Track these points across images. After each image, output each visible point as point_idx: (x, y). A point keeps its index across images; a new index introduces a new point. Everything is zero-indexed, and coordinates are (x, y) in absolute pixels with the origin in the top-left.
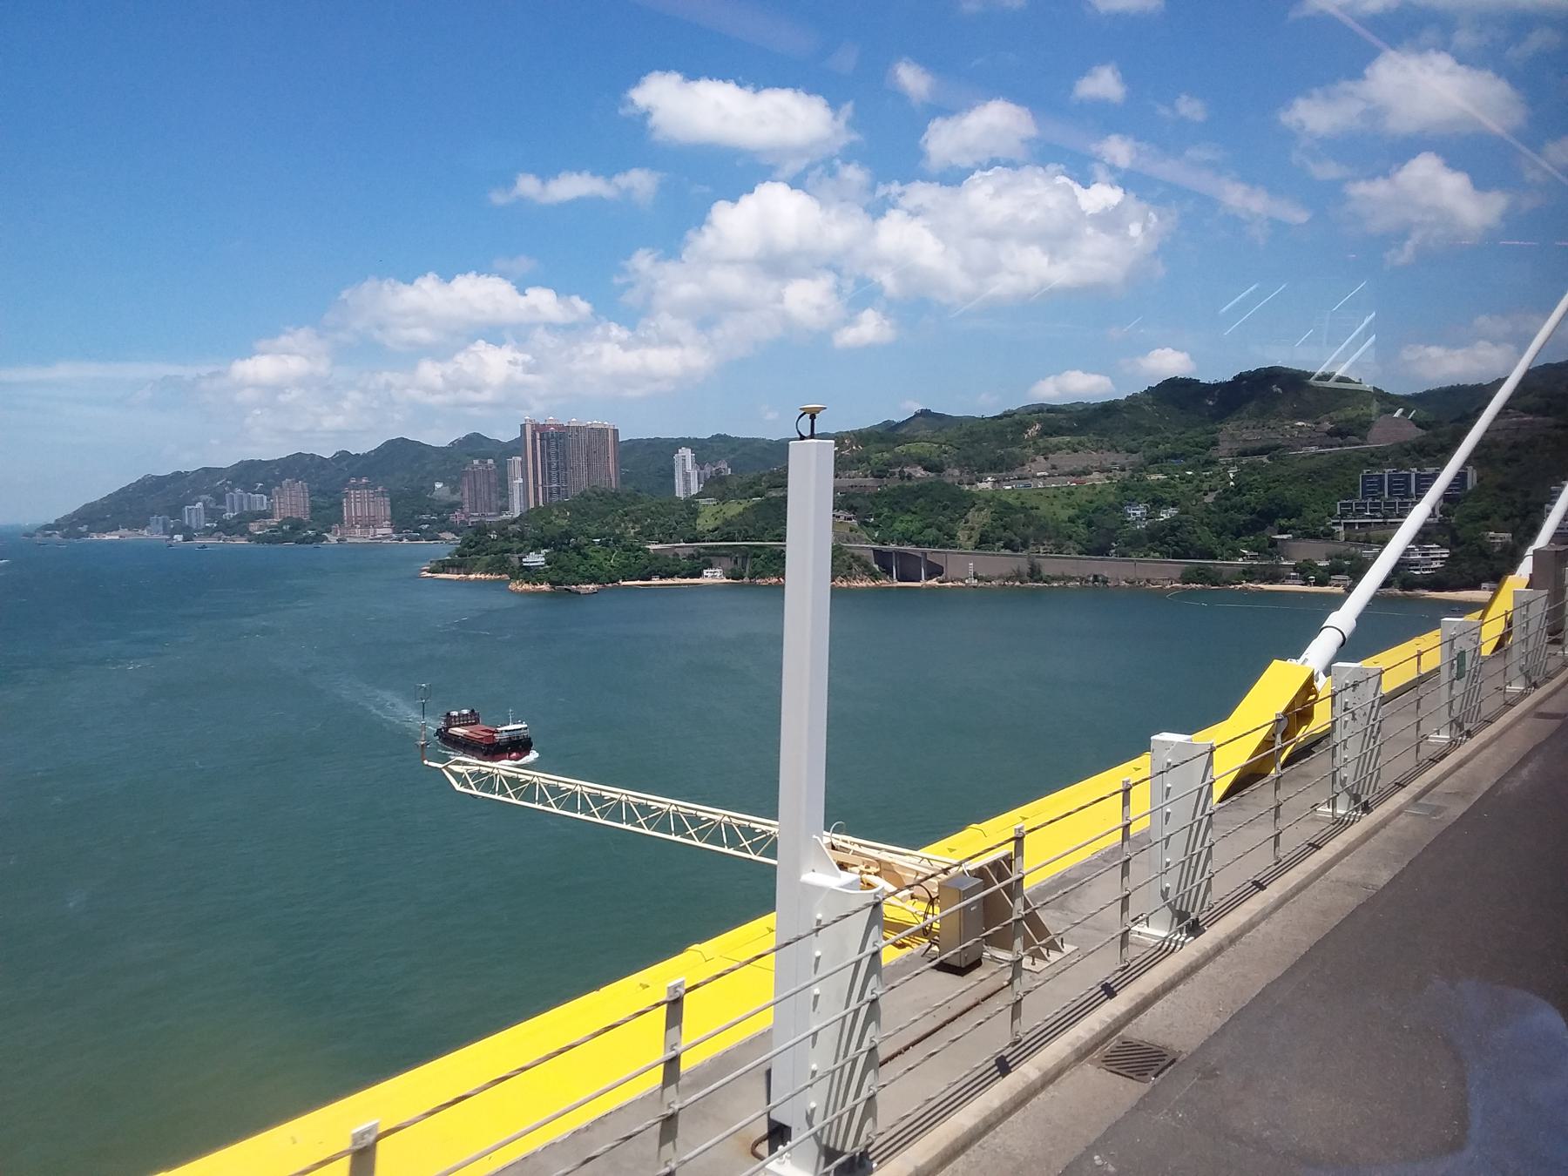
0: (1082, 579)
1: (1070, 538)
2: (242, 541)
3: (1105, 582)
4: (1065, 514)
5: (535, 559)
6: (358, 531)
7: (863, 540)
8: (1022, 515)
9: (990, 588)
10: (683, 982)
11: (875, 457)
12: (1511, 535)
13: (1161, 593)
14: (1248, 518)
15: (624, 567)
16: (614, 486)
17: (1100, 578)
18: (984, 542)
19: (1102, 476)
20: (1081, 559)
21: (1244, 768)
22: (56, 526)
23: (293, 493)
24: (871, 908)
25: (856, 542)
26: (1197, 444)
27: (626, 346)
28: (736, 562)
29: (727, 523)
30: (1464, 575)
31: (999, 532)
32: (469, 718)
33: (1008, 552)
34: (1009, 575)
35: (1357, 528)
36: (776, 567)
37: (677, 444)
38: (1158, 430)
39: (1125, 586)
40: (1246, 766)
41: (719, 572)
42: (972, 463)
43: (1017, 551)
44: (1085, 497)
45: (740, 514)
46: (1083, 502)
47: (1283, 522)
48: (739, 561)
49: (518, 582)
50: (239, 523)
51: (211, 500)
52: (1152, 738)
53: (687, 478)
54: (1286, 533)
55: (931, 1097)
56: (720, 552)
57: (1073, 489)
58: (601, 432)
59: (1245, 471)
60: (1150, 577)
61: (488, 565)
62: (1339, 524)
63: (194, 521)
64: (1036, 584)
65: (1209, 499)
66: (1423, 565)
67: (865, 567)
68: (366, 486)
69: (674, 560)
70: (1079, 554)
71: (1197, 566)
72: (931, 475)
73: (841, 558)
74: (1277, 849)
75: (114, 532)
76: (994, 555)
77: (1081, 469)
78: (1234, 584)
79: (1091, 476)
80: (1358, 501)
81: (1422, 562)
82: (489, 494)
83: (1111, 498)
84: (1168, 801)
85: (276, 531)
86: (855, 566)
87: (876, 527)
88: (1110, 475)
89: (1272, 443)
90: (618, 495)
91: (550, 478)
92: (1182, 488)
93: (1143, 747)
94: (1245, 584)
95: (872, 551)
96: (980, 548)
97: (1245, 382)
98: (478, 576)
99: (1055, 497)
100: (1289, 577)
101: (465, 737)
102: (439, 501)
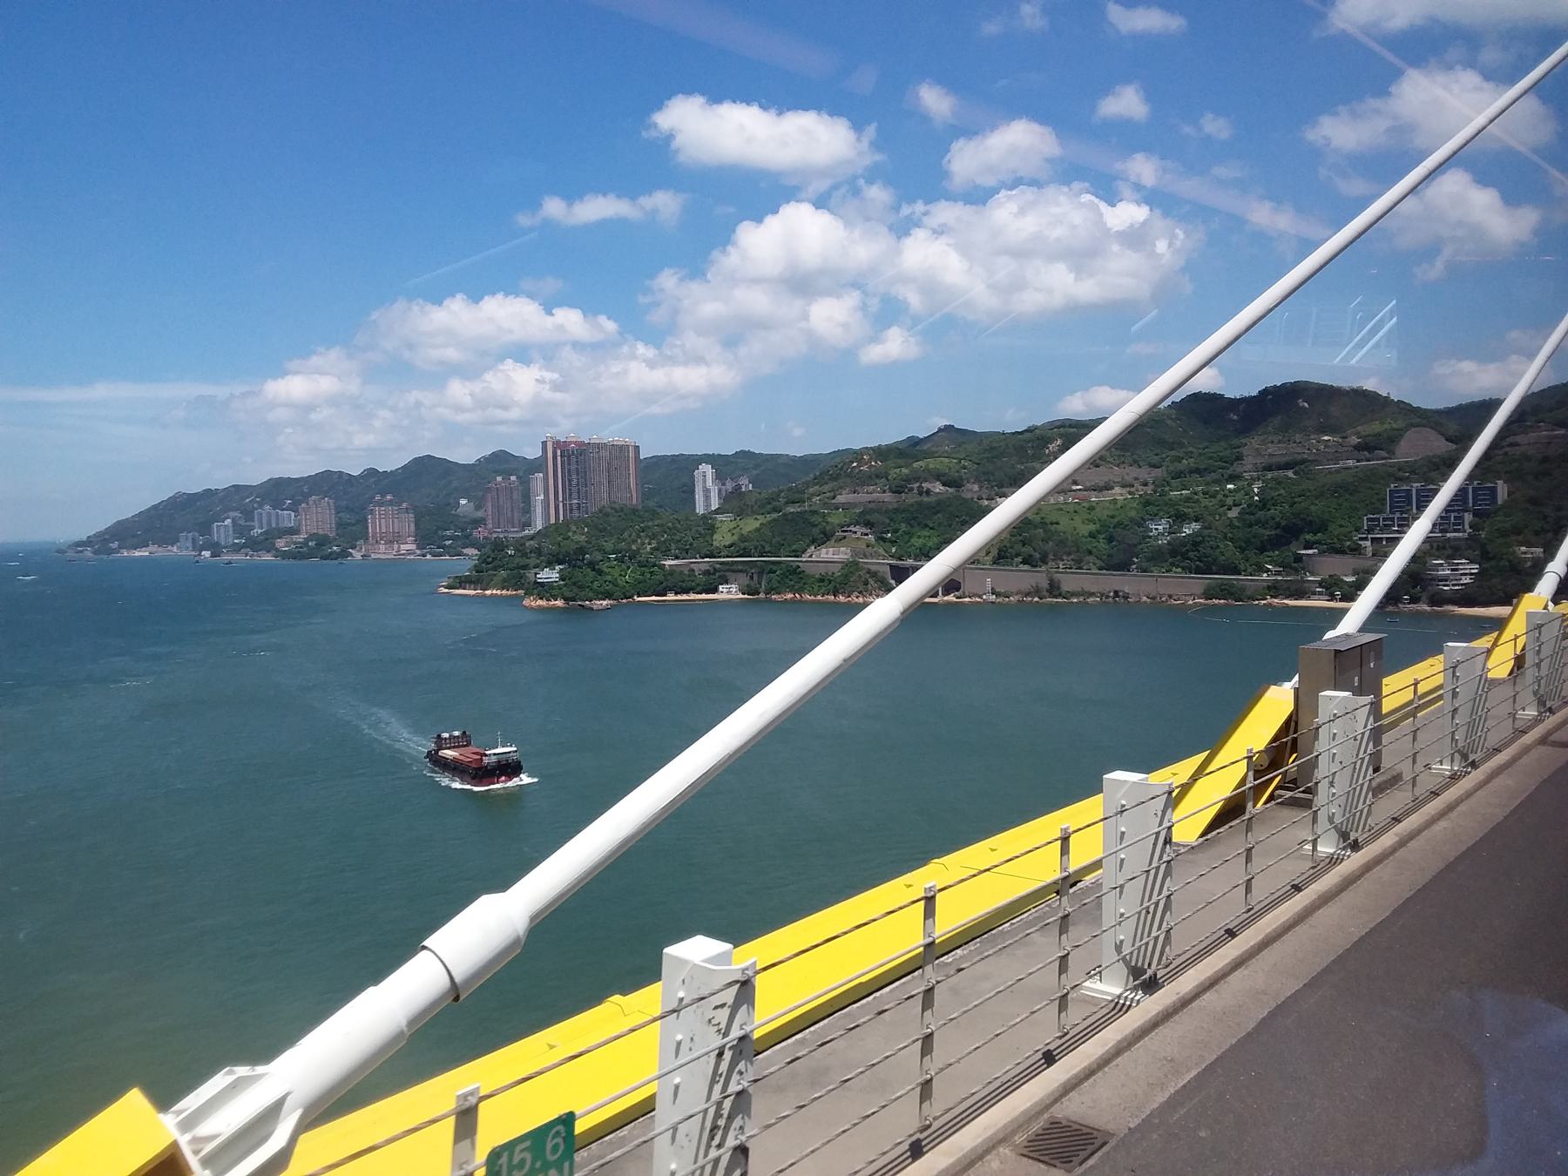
0: (1102, 595)
1: (1090, 553)
2: (268, 557)
3: (1126, 597)
4: (1085, 529)
5: (549, 575)
6: (382, 547)
7: (880, 556)
8: (1041, 530)
9: (1007, 603)
10: (478, 1088)
11: (894, 473)
13: (1184, 607)
14: (1272, 533)
15: (639, 583)
16: (634, 502)
17: (1121, 594)
19: (1124, 491)
20: (1101, 574)
21: (1228, 801)
22: (89, 542)
23: (320, 510)
24: (738, 985)
25: (872, 557)
27: (651, 364)
28: (752, 578)
29: (743, 539)
31: (1018, 547)
32: (460, 740)
33: (1026, 567)
34: (1028, 591)
35: (1384, 543)
36: (792, 583)
37: (697, 460)
38: (1182, 445)
39: (1145, 602)
41: (734, 588)
42: (992, 478)
43: (1036, 566)
44: (1106, 512)
45: (757, 530)
46: (1105, 517)
47: (1308, 537)
48: (755, 577)
49: (532, 598)
50: (267, 539)
51: (240, 517)
52: (1104, 776)
53: (707, 493)
54: (1311, 548)
55: (857, 1169)
56: (735, 567)
57: (1094, 504)
58: (623, 449)
59: (1269, 485)
61: (505, 580)
62: (1366, 539)
63: (223, 536)
64: (1055, 600)
65: (1234, 513)
66: (1452, 580)
67: (882, 583)
68: (391, 503)
69: (689, 576)
70: (1099, 569)
71: (1219, 581)
72: (950, 490)
73: (857, 574)
75: (144, 549)
76: (1012, 571)
77: (1102, 484)
78: (1257, 600)
79: (1113, 491)
80: (1385, 515)
82: (512, 511)
83: (1133, 514)
84: (1122, 847)
85: (301, 547)
86: (871, 581)
87: (893, 542)
88: (1132, 490)
90: (637, 510)
91: (570, 495)
92: (1205, 502)
93: (1094, 787)
94: (1269, 600)
96: (998, 564)
98: (494, 592)
99: (1075, 512)
100: (1314, 593)
101: (455, 760)
102: (464, 517)
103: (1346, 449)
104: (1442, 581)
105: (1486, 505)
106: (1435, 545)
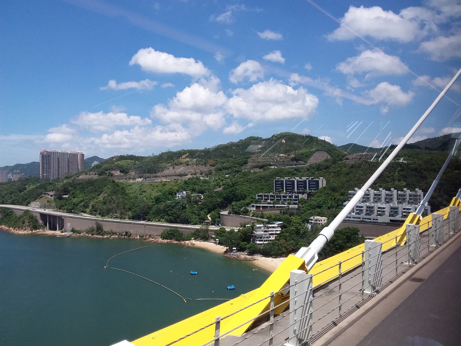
12: (327, 219)
18: (94, 211)
26: (238, 163)
27: (161, 132)
30: (280, 247)
35: (261, 209)
40: (258, 318)
60: (150, 233)
68: (18, 173)
86: (27, 222)
89: (268, 163)
94: (194, 242)
95: (39, 214)
96: (91, 214)
97: (275, 138)
100: (212, 238)
103: (288, 160)
104: (258, 238)
105: (314, 190)
106: (282, 211)
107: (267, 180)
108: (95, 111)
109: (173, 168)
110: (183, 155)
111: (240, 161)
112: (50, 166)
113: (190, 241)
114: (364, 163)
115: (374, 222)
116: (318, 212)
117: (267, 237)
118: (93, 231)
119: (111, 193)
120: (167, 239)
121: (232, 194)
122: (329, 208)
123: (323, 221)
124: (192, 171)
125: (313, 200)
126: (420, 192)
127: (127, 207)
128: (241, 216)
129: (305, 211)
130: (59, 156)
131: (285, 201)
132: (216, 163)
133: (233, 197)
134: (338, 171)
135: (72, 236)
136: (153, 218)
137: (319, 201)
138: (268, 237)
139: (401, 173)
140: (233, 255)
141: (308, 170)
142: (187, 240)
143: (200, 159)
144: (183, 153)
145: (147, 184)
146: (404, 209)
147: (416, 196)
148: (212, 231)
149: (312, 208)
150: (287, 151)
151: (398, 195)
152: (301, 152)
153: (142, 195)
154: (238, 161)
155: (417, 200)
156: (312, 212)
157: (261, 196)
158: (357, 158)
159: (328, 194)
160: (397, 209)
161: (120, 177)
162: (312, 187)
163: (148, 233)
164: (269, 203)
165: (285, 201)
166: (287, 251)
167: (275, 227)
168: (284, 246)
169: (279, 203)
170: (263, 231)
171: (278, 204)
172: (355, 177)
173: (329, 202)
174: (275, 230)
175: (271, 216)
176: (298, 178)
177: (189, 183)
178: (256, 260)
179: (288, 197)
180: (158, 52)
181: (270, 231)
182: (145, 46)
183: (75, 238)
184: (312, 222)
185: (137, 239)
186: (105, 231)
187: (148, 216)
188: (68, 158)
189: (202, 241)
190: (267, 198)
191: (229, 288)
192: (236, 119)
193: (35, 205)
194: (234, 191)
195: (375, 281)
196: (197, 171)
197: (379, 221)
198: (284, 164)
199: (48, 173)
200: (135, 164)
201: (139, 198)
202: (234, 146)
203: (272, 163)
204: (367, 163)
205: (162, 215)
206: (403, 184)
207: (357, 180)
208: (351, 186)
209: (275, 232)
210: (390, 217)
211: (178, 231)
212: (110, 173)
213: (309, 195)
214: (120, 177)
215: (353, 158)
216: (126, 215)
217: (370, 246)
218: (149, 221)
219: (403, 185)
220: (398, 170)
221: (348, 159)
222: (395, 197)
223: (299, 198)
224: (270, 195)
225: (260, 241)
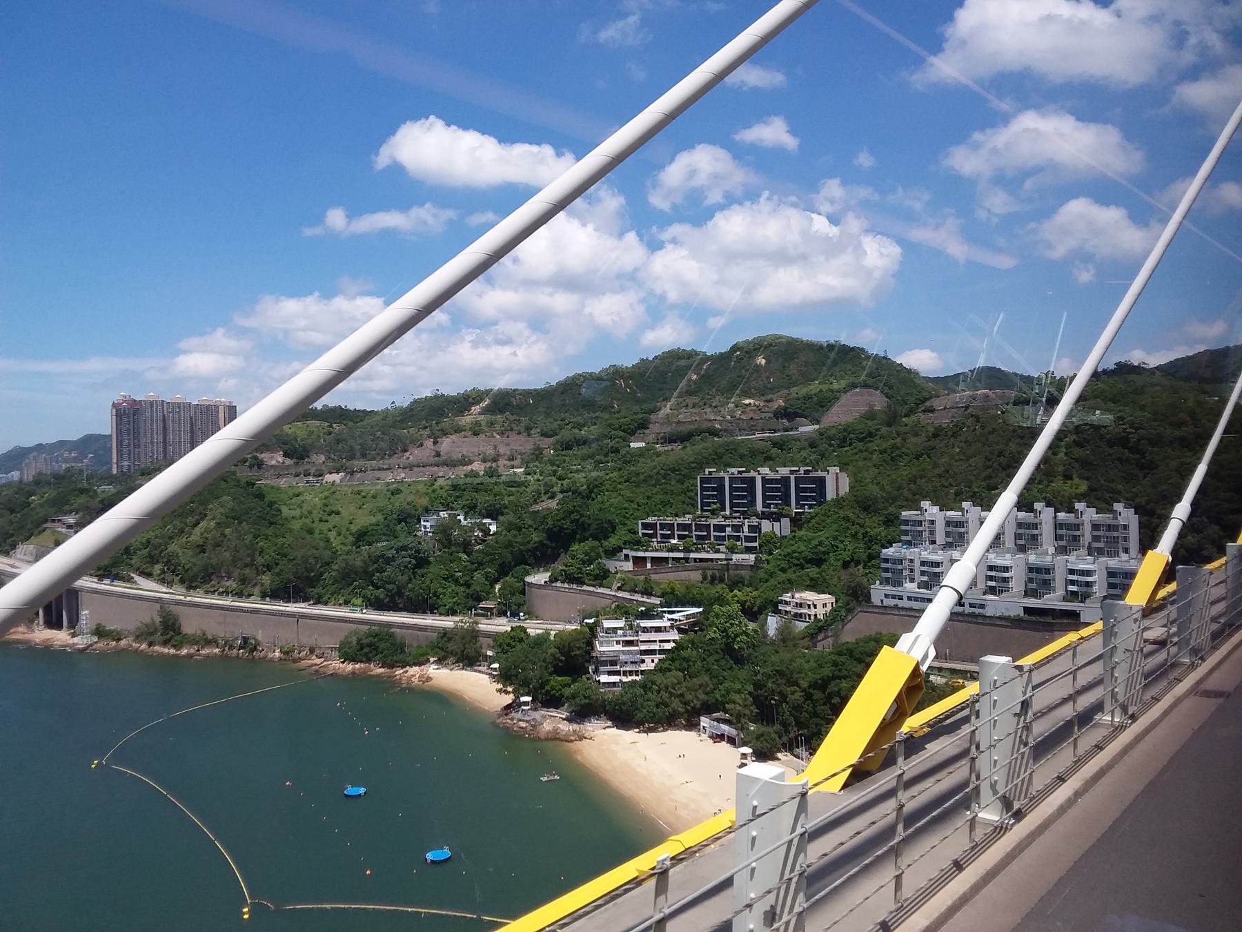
27: (475, 344)
35: (649, 566)
60: (312, 641)
74: (899, 893)
81: (623, 658)
89: (705, 425)
97: (738, 353)
99: (373, 497)
103: (763, 415)
104: (604, 663)
105: (811, 506)
106: (709, 573)
107: (684, 475)
108: (297, 292)
109: (435, 443)
110: (473, 404)
111: (627, 419)
112: (139, 441)
113: (423, 667)
114: (970, 422)
115: (973, 615)
116: (812, 579)
117: (632, 662)
118: (151, 634)
119: (227, 517)
120: (354, 660)
121: (572, 522)
122: (846, 565)
123: (820, 606)
124: (488, 452)
125: (800, 539)
126: (1127, 516)
127: (260, 560)
128: (585, 588)
129: (771, 575)
130: (165, 413)
131: (719, 543)
132: (561, 428)
133: (573, 530)
134: (894, 447)
135: (94, 647)
136: (332, 594)
137: (815, 542)
138: (636, 663)
139: (1077, 452)
140: (521, 720)
141: (813, 445)
142: (415, 664)
143: (515, 417)
144: (473, 399)
145: (346, 489)
146: (1072, 572)
147: (1115, 528)
148: (488, 635)
149: (796, 565)
150: (770, 389)
151: (1058, 526)
152: (804, 391)
153: (327, 521)
154: (621, 420)
155: (1115, 540)
156: (794, 577)
157: (651, 526)
158: (957, 407)
159: (847, 519)
160: (1048, 571)
161: (280, 471)
162: (806, 498)
163: (308, 640)
164: (674, 549)
165: (719, 543)
166: (686, 709)
167: (663, 629)
168: (679, 693)
169: (704, 548)
170: (619, 641)
171: (697, 550)
172: (935, 466)
173: (849, 547)
174: (658, 639)
175: (673, 589)
176: (765, 470)
177: (463, 487)
178: (586, 738)
179: (730, 529)
180: (454, 127)
181: (641, 642)
182: (418, 113)
183: (103, 655)
184: (788, 609)
185: (272, 660)
186: (186, 634)
187: (318, 590)
188: (191, 418)
189: (459, 666)
190: (669, 532)
191: (430, 856)
192: (673, 307)
193: (25, 555)
194: (577, 511)
195: (1012, 782)
196: (503, 450)
197: (989, 612)
198: (754, 428)
199: (133, 460)
200: (330, 433)
201: (317, 531)
202: (622, 377)
203: (718, 426)
204: (978, 421)
205: (356, 586)
206: (1076, 488)
207: (940, 476)
208: (921, 494)
209: (660, 646)
210: (1026, 600)
211: (392, 635)
212: (256, 458)
213: (796, 522)
214: (280, 471)
215: (945, 408)
216: (256, 585)
217: (994, 675)
218: (318, 601)
219: (1079, 491)
220: (1067, 445)
221: (932, 411)
222: (1047, 530)
223: (760, 532)
224: (678, 524)
225: (610, 673)
